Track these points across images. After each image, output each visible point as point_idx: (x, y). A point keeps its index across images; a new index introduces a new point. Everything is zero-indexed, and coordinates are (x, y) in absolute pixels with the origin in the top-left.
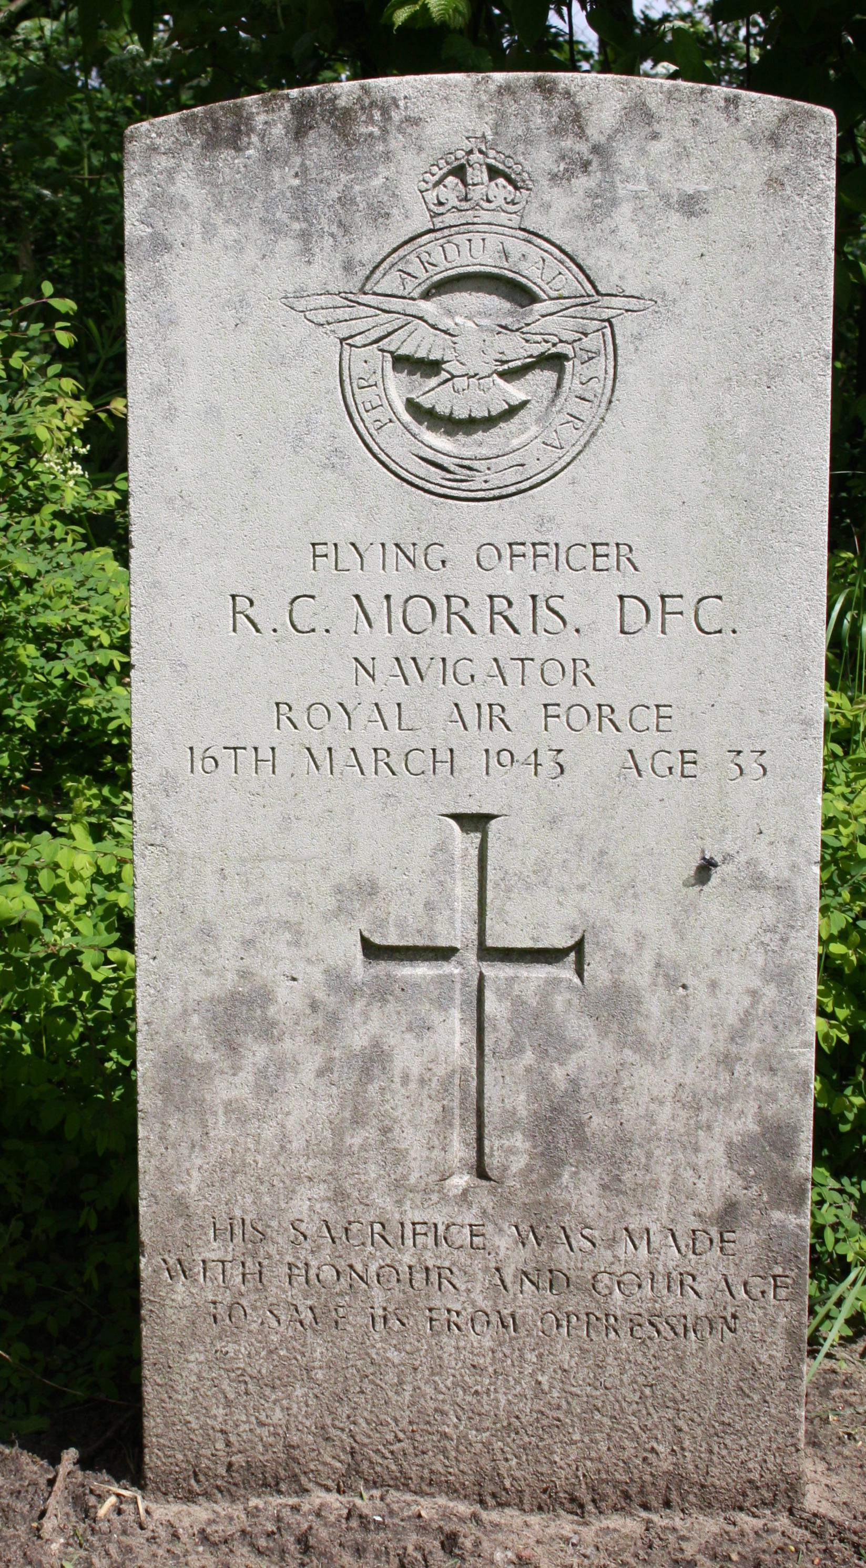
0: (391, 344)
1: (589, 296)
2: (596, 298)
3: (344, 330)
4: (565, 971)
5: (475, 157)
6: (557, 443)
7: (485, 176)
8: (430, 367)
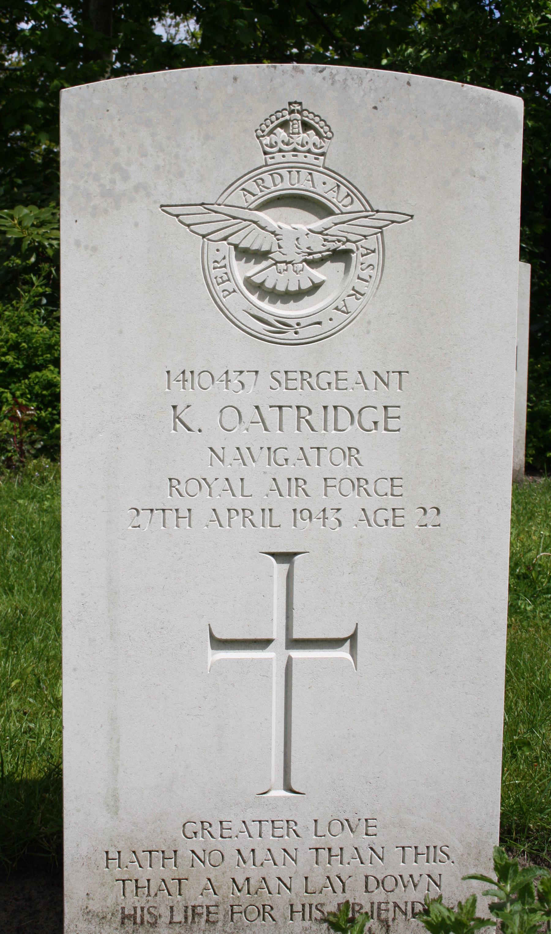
0: (233, 239)
1: (368, 211)
3: (203, 229)
6: (344, 309)
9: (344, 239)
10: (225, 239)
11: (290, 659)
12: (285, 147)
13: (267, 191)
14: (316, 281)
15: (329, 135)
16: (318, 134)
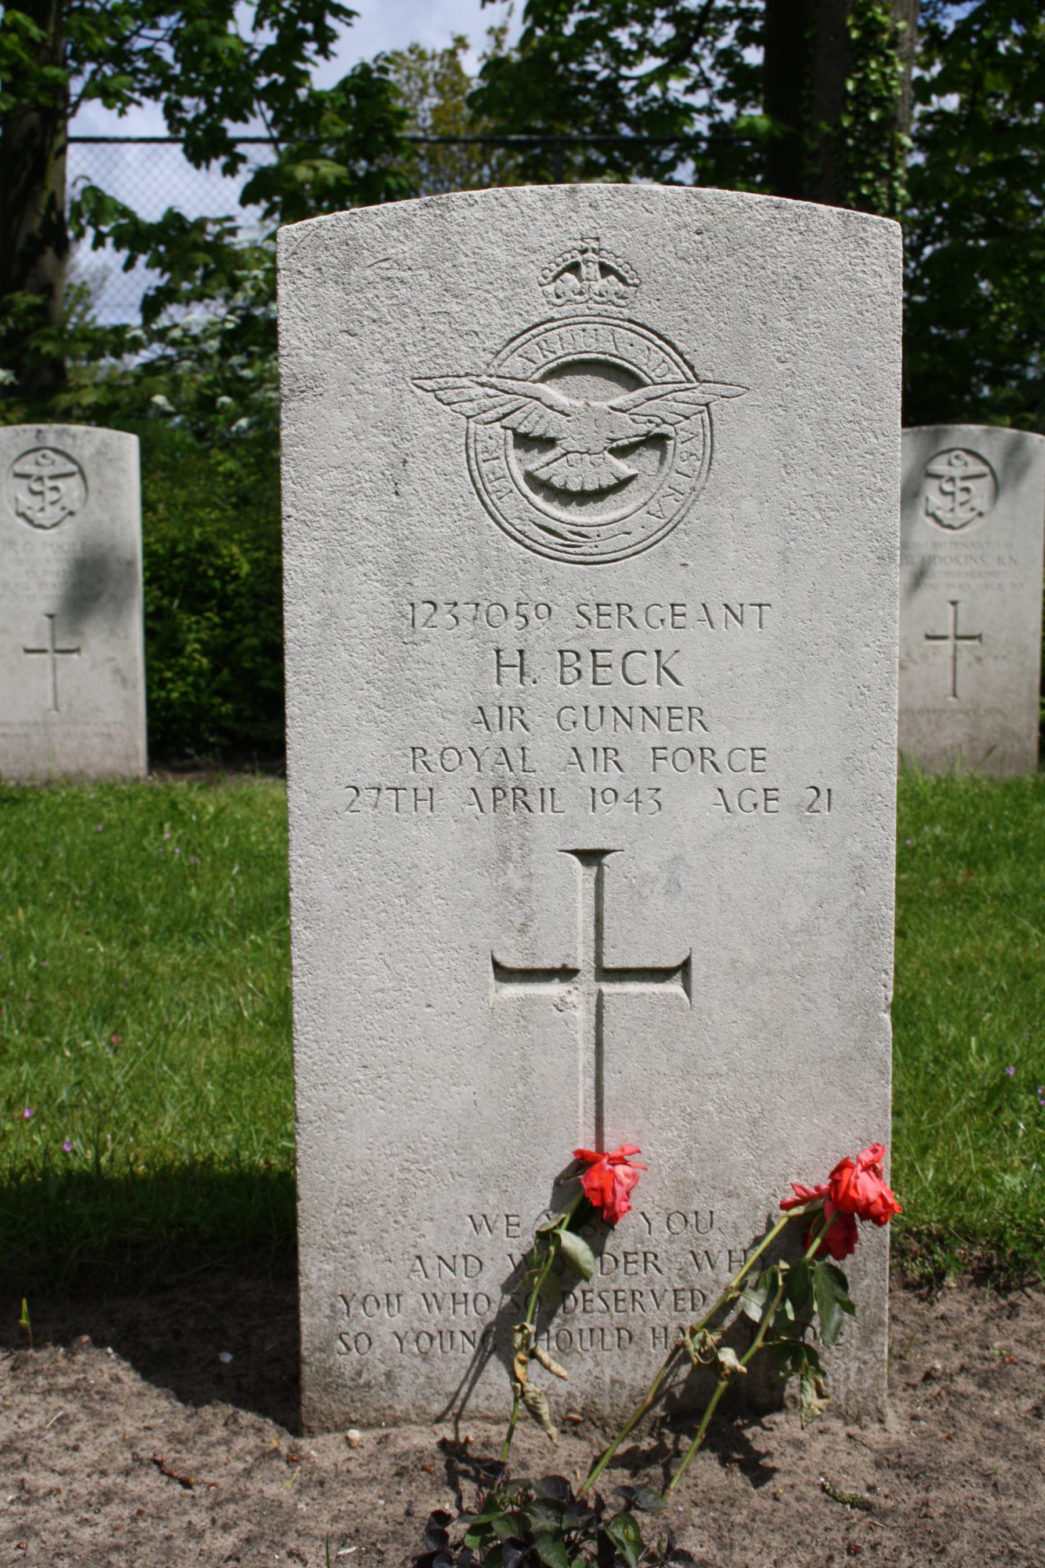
2: (696, 384)
4: (674, 988)
5: (590, 255)
7: (598, 275)
8: (547, 443)
9: (658, 420)
10: (498, 420)
11: (600, 995)
12: (578, 298)
14: (623, 477)
15: (637, 281)
16: (622, 280)
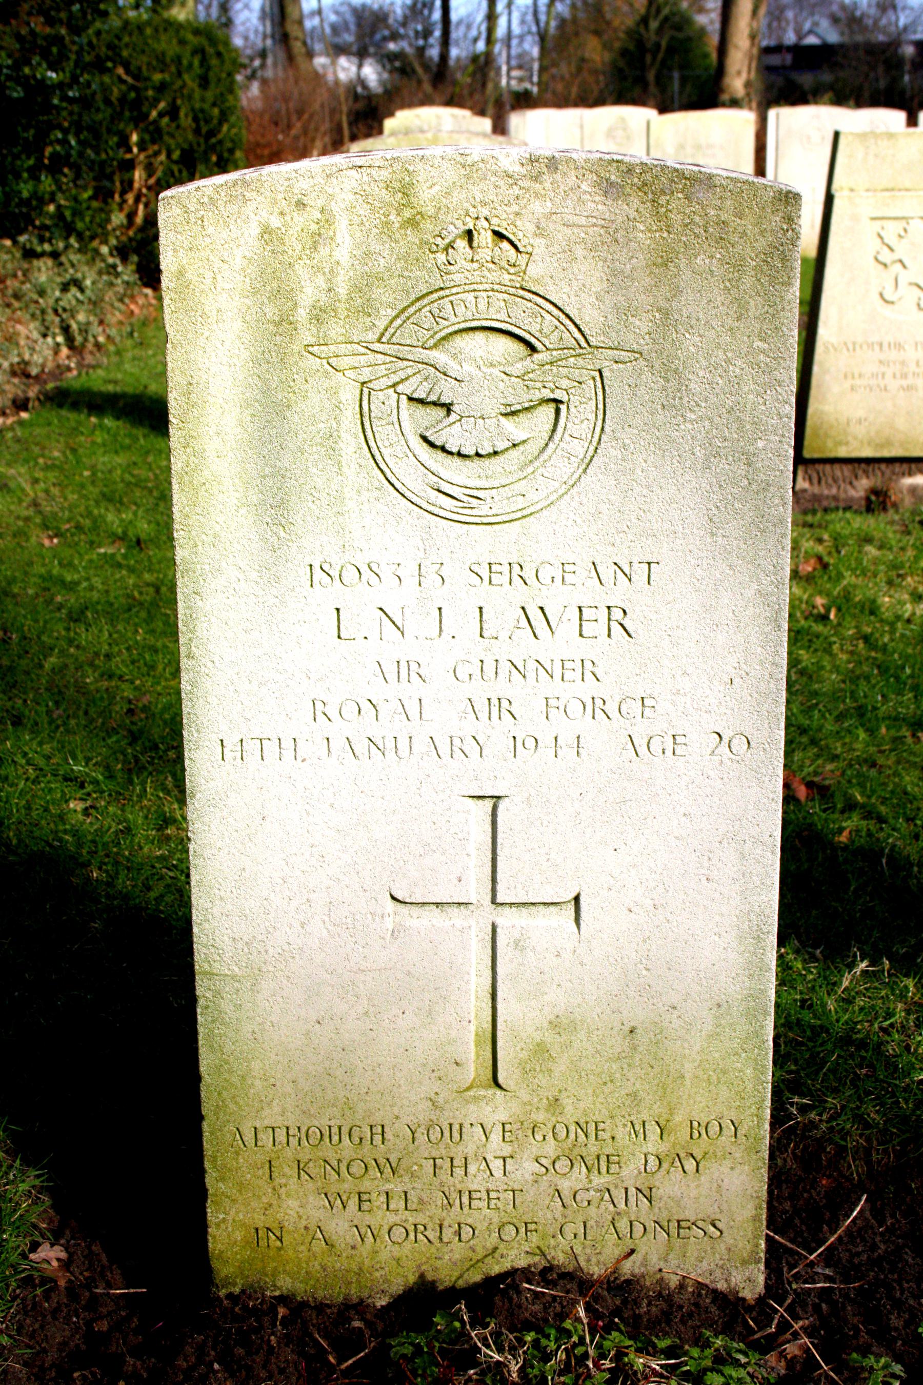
2: (590, 350)
10: (394, 385)
13: (446, 323)
